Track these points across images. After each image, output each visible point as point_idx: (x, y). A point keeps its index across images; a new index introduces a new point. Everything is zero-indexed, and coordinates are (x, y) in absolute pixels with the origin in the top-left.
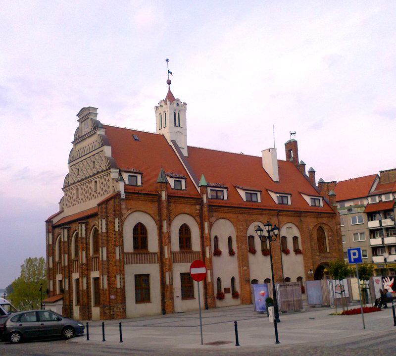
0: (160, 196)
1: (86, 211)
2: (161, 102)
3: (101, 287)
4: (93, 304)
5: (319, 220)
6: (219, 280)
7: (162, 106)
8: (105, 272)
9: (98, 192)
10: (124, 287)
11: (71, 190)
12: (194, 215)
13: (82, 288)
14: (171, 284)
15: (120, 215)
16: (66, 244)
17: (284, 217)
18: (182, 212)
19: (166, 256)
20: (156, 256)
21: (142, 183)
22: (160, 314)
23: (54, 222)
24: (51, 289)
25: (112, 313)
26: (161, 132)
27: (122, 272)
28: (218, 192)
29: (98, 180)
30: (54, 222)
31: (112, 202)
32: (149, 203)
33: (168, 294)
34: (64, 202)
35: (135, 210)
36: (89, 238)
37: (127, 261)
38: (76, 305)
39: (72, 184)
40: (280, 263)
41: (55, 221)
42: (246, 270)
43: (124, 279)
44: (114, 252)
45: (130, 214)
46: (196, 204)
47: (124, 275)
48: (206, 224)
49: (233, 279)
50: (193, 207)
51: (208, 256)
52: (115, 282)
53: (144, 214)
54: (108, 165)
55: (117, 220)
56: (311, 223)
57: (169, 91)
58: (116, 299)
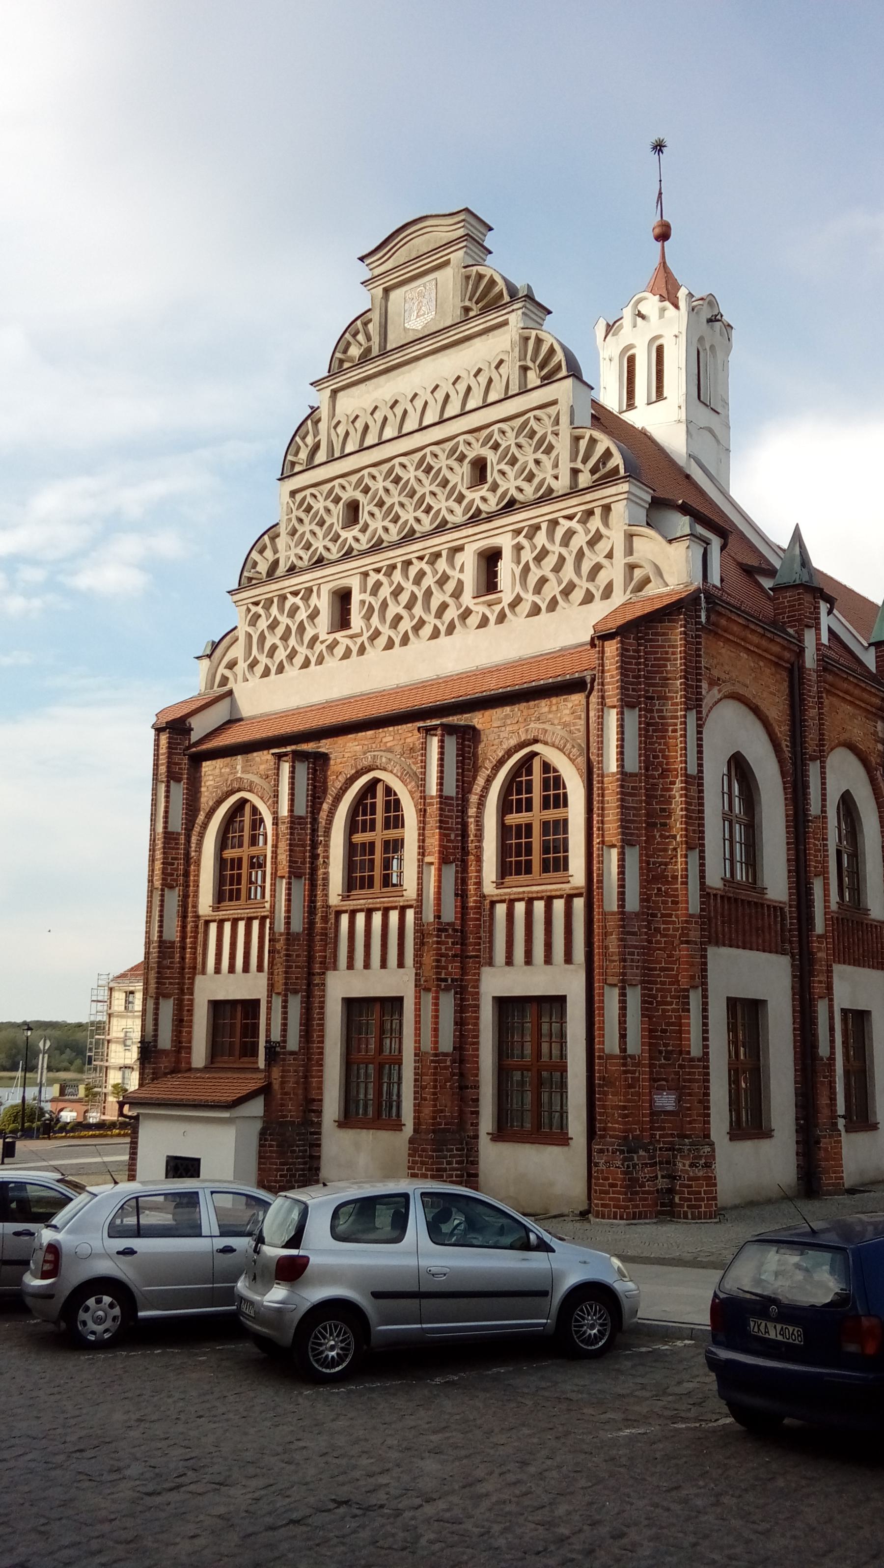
1: (449, 680)
4: (486, 1122)
7: (643, 317)
8: (634, 974)
9: (507, 597)
11: (291, 600)
12: (874, 760)
18: (844, 736)
19: (819, 927)
21: (722, 580)
22: (786, 1198)
23: (195, 737)
24: (165, 1041)
27: (701, 980)
29: (506, 542)
30: (195, 737)
32: (768, 671)
34: (237, 651)
35: (727, 688)
38: (347, 1121)
39: (292, 570)
41: (200, 726)
45: (716, 703)
52: (681, 1030)
53: (751, 717)
54: (593, 471)
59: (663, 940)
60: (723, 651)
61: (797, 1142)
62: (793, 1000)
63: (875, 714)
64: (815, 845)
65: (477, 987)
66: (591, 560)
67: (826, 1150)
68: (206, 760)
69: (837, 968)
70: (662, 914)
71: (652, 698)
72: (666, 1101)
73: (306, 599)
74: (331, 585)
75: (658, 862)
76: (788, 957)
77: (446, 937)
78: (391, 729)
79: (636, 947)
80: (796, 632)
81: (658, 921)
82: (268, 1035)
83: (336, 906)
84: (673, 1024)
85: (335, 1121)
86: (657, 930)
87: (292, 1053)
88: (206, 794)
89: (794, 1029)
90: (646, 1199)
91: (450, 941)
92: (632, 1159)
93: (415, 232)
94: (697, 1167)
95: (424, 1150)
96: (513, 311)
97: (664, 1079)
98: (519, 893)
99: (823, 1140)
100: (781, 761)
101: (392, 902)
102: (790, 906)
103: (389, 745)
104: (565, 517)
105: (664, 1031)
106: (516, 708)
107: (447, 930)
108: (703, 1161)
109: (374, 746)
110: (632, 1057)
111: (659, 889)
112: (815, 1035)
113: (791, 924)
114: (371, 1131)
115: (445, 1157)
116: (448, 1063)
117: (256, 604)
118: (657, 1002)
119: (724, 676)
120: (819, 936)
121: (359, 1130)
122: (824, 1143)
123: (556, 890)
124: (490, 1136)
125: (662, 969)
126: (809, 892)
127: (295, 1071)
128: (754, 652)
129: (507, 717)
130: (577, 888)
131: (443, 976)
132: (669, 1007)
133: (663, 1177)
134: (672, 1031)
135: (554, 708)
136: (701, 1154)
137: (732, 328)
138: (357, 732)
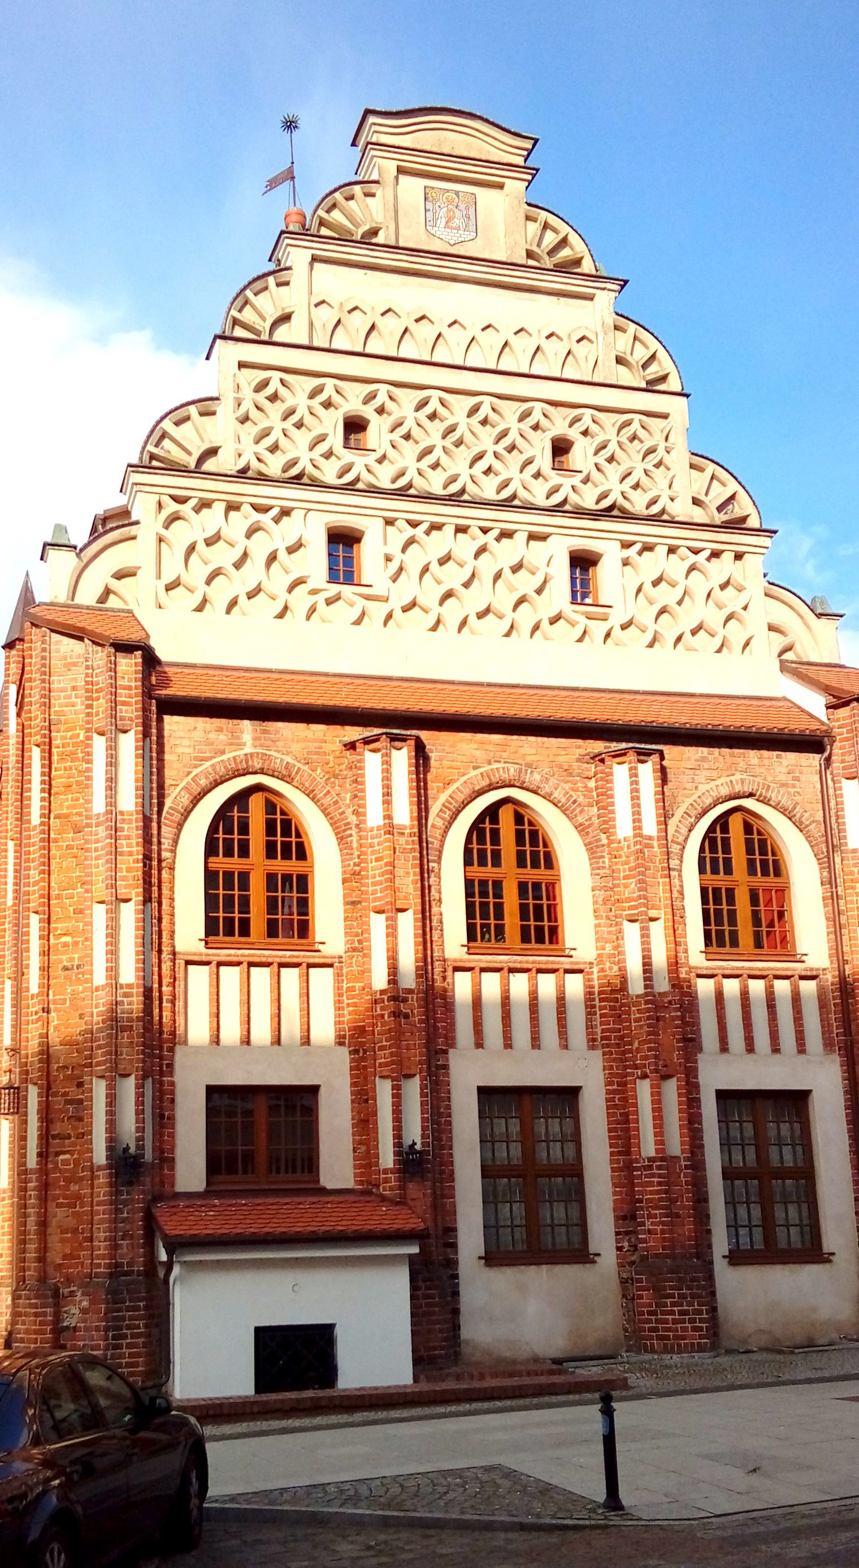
4: (720, 1244)
38: (493, 1258)
66: (439, 582)
68: (172, 714)
78: (532, 739)
82: (398, 1135)
83: (455, 961)
85: (480, 1258)
88: (175, 765)
93: (461, 125)
95: (693, 1279)
96: (604, 289)
98: (738, 968)
101: (553, 963)
103: (529, 759)
104: (688, 548)
106: (716, 751)
109: (505, 755)
114: (544, 1267)
121: (523, 1267)
123: (787, 969)
124: (727, 1260)
129: (703, 759)
130: (812, 970)
135: (766, 762)
138: (475, 732)
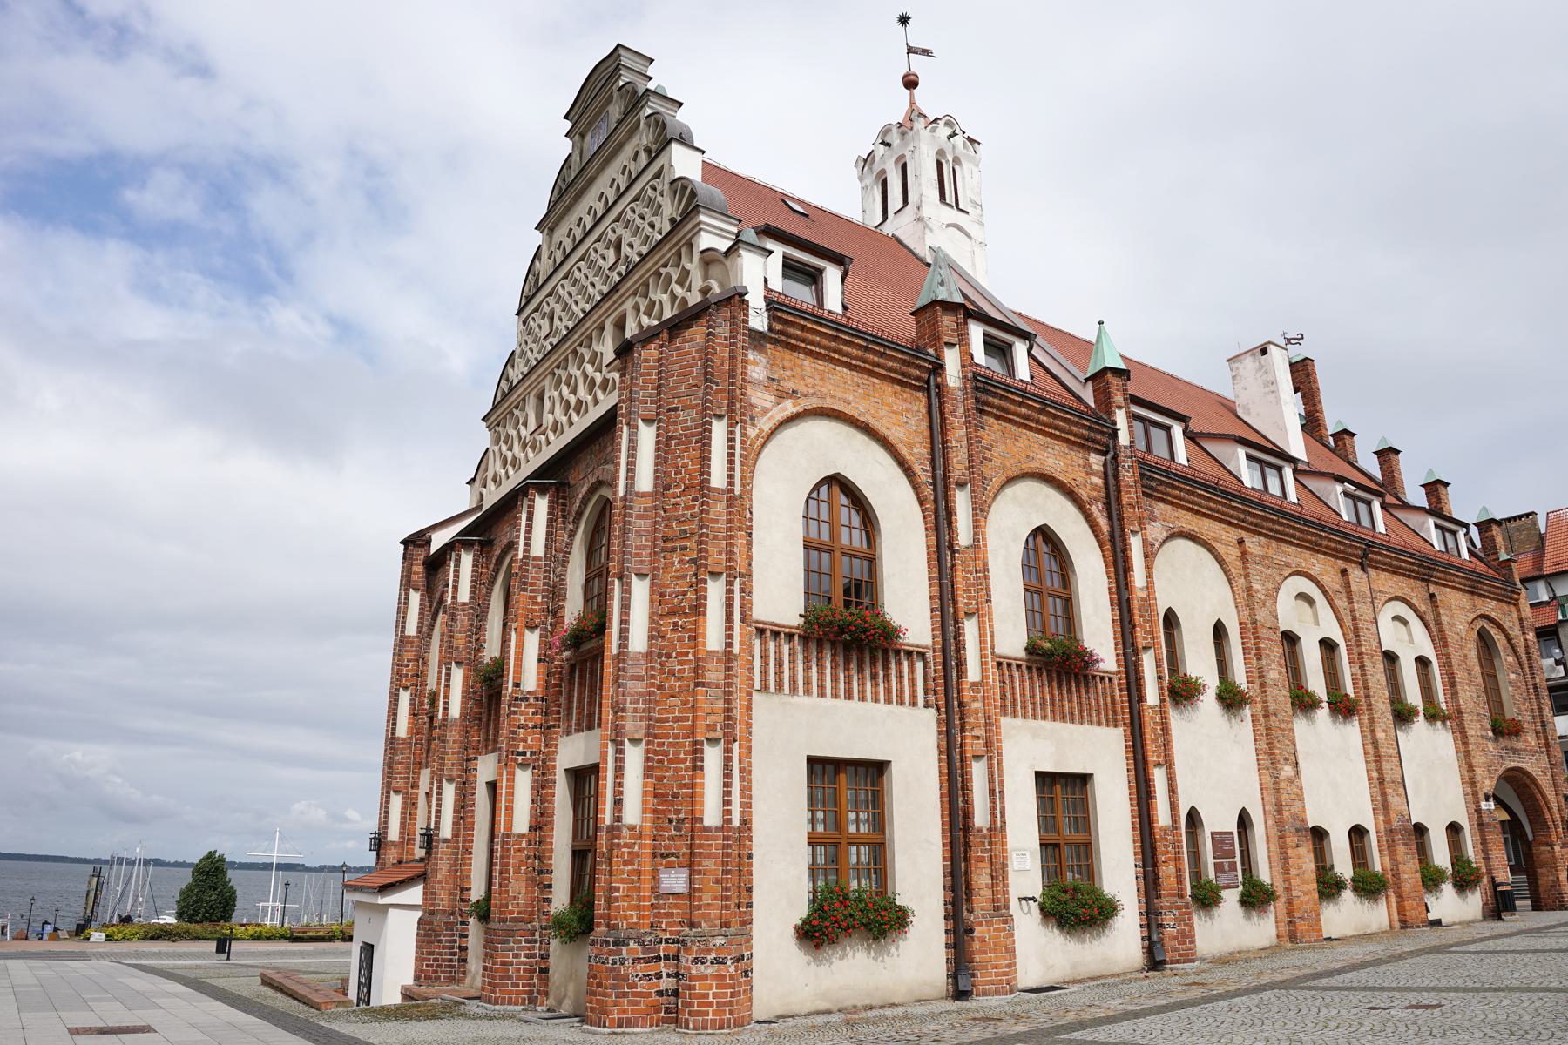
0: (939, 368)
2: (886, 131)
3: (607, 817)
5: (1478, 601)
6: (1193, 818)
8: (633, 726)
10: (746, 821)
12: (1084, 494)
13: (509, 823)
14: (997, 831)
15: (737, 413)
16: (463, 620)
17: (1383, 575)
19: (973, 673)
20: (919, 665)
24: (394, 834)
25: (666, 983)
26: (888, 229)
27: (732, 731)
28: (1153, 430)
31: (697, 333)
33: (981, 878)
35: (813, 403)
36: (565, 563)
37: (765, 672)
40: (1396, 761)
42: (1291, 781)
43: (746, 772)
44: (699, 608)
46: (1086, 445)
47: (747, 753)
48: (1135, 544)
49: (1244, 820)
50: (1077, 456)
51: (1152, 696)
52: (693, 792)
53: (860, 439)
55: (719, 430)
56: (1459, 609)
57: (912, 103)
58: (691, 894)
59: (677, 684)
60: (806, 363)
61: (947, 932)
62: (940, 760)
63: (1082, 446)
64: (965, 578)
65: (554, 760)
67: (982, 941)
69: (1006, 722)
70: (678, 653)
71: (676, 409)
72: (675, 880)
73: (523, 410)
74: (534, 392)
75: (673, 592)
76: (933, 711)
77: (527, 706)
79: (641, 694)
80: (936, 350)
81: (672, 662)
84: (685, 786)
86: (671, 672)
87: (446, 841)
89: (942, 796)
90: (637, 1003)
91: (531, 710)
92: (619, 953)
94: (703, 963)
97: (673, 855)
99: (977, 929)
100: (916, 488)
102: (934, 651)
105: (675, 795)
107: (527, 699)
108: (713, 955)
110: (632, 828)
111: (675, 624)
112: (967, 801)
113: (935, 671)
115: (512, 949)
116: (524, 845)
117: (498, 425)
118: (669, 760)
119: (805, 390)
120: (973, 684)
122: (978, 932)
125: (676, 720)
126: (958, 634)
127: (448, 859)
128: (856, 366)
131: (521, 749)
132: (682, 766)
133: (669, 975)
134: (686, 795)
136: (711, 947)
137: (979, 143)
